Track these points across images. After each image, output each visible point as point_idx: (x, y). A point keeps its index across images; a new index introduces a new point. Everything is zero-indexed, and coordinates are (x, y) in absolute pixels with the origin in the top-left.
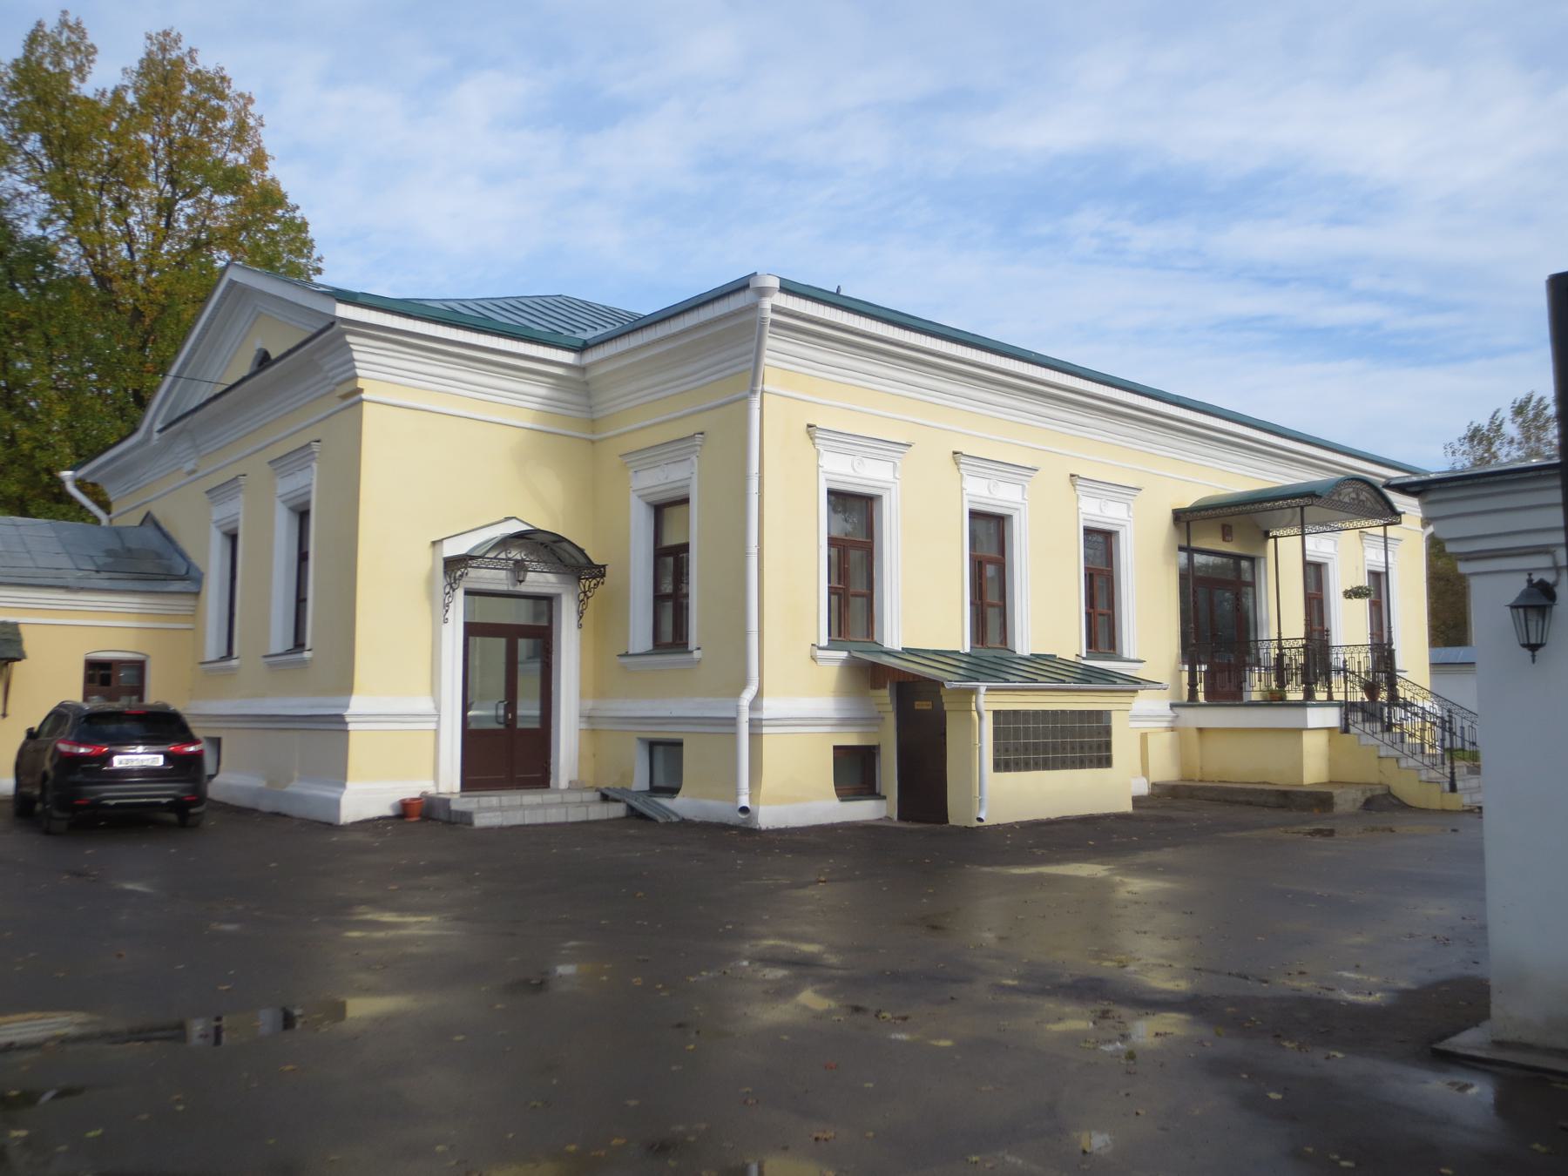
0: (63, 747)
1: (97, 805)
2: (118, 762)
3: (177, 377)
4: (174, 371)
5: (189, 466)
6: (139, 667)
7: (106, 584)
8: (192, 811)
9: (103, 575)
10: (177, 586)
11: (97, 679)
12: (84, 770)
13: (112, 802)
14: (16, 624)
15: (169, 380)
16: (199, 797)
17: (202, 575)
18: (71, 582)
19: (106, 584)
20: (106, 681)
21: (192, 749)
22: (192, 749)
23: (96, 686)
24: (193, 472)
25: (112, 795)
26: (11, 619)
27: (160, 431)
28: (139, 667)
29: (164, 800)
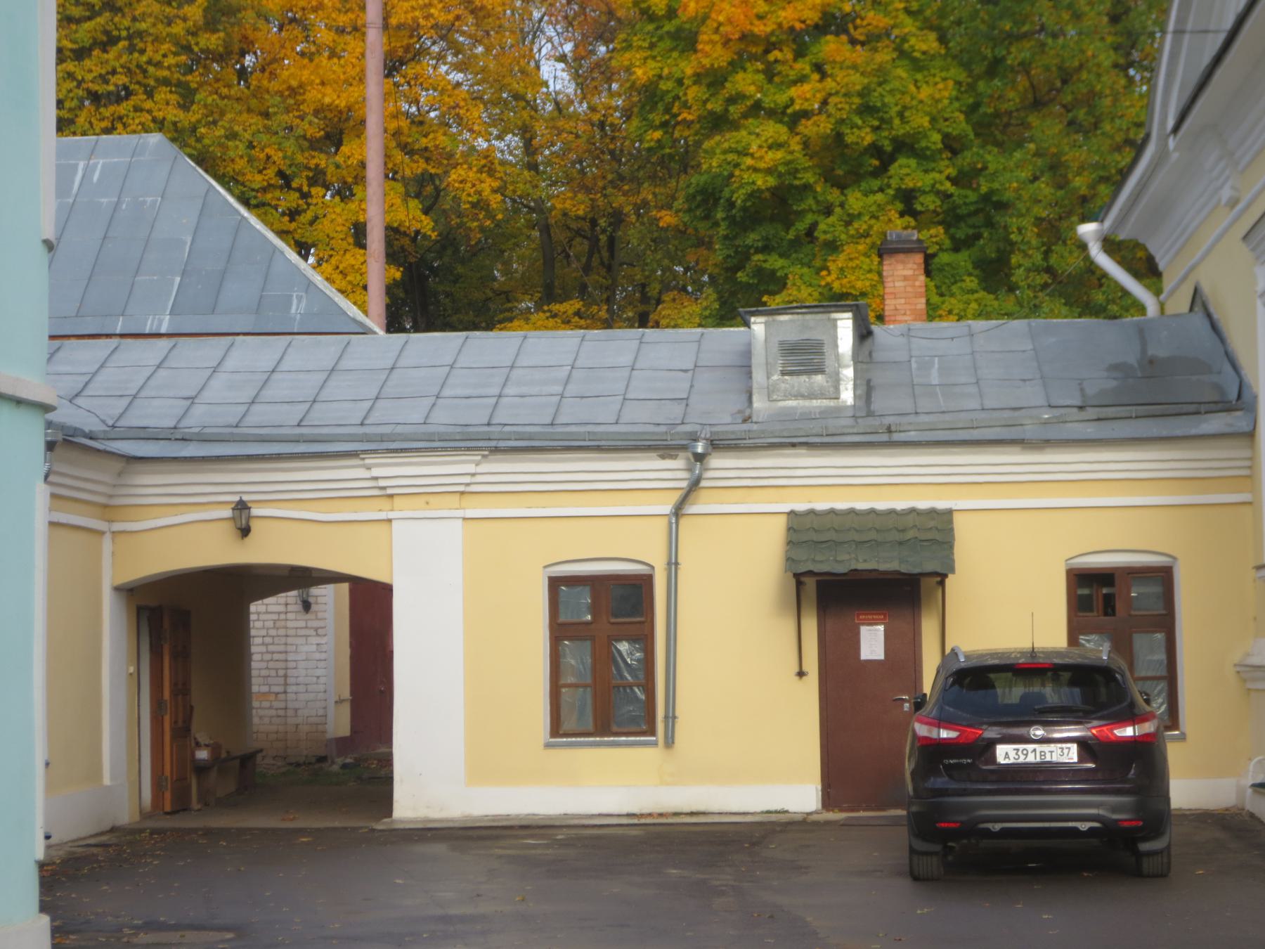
0: (922, 730)
1: (972, 831)
2: (1006, 754)
3: (1179, 32)
4: (1171, 26)
5: (1226, 193)
6: (1163, 577)
7: (1090, 430)
8: (1145, 847)
9: (1091, 413)
10: (1215, 423)
11: (1098, 603)
12: (949, 768)
13: (997, 827)
14: (950, 512)
15: (1169, 38)
16: (1154, 813)
17: (1255, 397)
18: (1030, 431)
19: (1090, 430)
20: (1109, 606)
21: (1129, 732)
22: (1129, 732)
23: (1095, 617)
24: (1233, 203)
25: (1000, 813)
26: (941, 505)
27: (1176, 129)
28: (1163, 577)
29: (1084, 826)
